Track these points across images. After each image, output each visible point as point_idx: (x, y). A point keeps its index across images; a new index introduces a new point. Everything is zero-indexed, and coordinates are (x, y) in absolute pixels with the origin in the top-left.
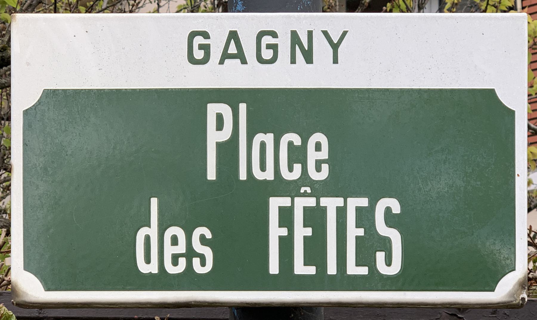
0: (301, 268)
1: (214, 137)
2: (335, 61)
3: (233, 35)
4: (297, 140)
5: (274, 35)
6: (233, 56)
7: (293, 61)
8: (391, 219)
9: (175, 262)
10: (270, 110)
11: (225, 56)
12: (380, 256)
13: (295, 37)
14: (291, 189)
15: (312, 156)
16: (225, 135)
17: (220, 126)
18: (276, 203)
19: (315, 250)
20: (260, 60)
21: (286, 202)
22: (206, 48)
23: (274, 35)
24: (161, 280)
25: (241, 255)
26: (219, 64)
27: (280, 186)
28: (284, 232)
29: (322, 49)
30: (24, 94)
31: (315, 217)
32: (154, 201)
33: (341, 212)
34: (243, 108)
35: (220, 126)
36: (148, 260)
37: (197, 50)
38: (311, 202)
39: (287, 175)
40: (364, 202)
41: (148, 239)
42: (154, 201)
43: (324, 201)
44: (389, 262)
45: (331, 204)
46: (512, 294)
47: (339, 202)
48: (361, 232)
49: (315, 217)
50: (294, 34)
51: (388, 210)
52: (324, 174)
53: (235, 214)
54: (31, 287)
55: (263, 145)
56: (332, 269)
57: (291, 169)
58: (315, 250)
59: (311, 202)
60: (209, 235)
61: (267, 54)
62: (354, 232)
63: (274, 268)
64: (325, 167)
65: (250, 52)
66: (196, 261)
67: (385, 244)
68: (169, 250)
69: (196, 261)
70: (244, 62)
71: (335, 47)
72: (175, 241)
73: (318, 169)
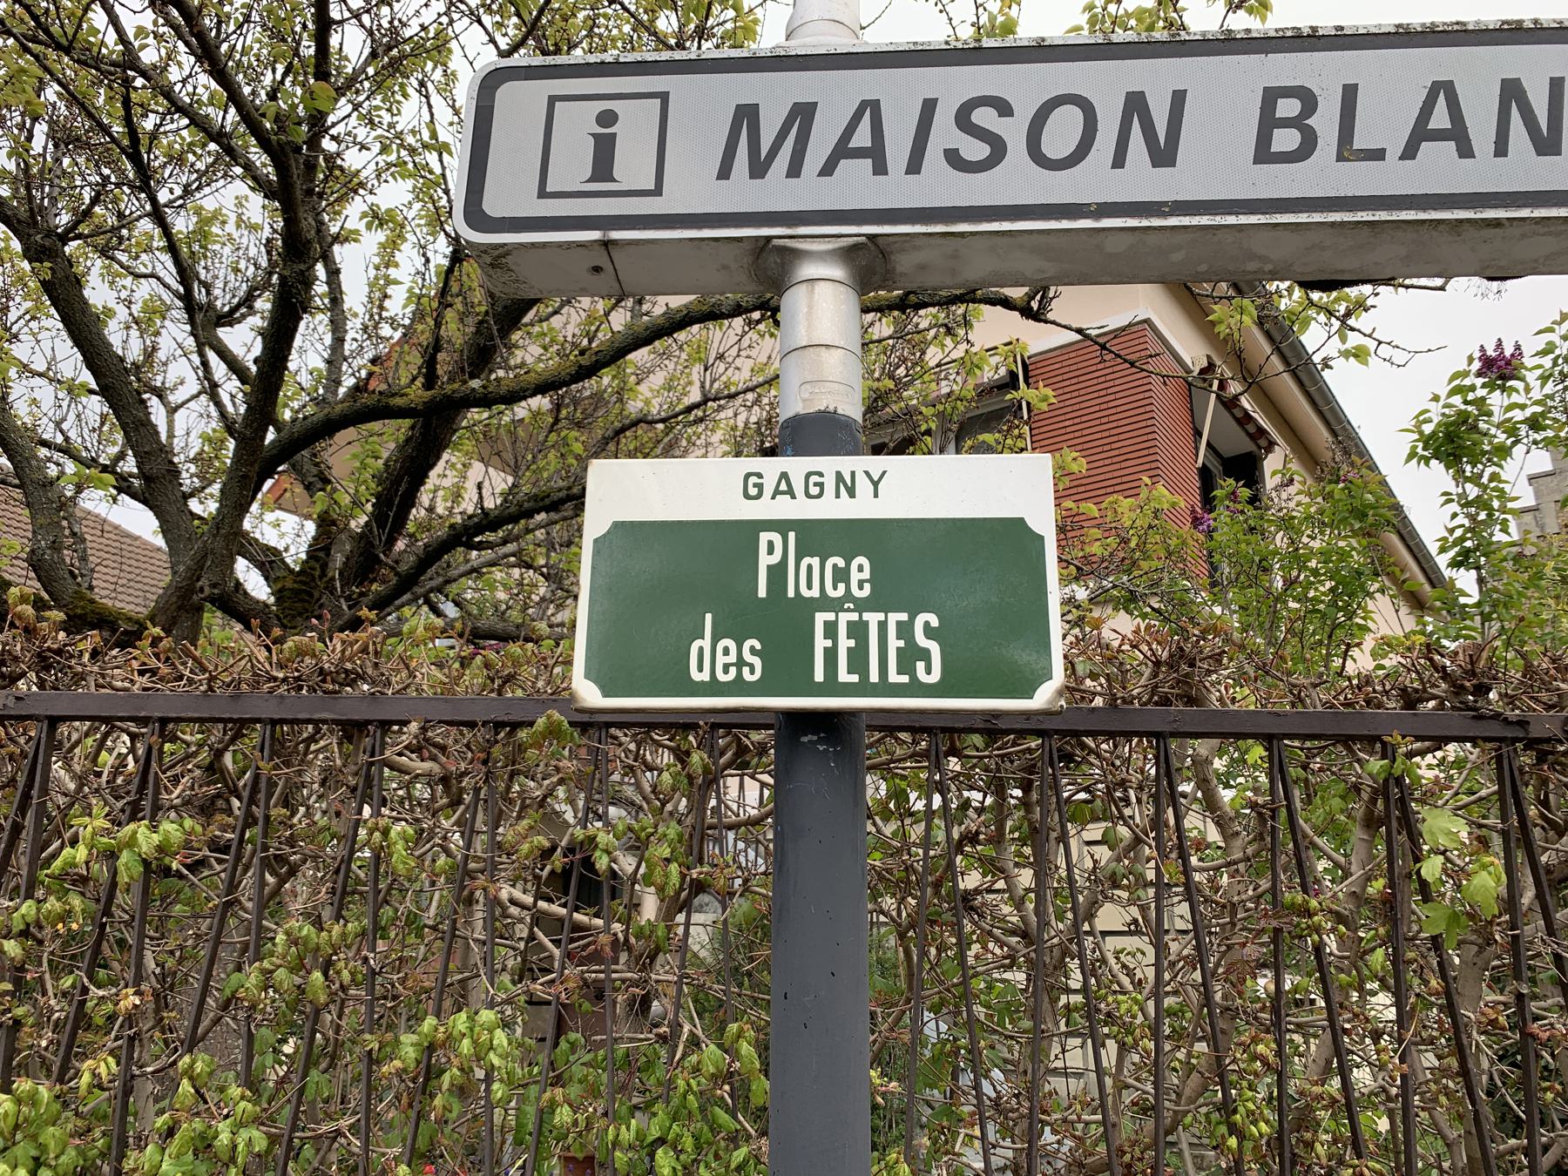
0: (844, 676)
1: (765, 561)
2: (876, 496)
3: (784, 475)
4: (841, 563)
5: (821, 474)
6: (783, 493)
7: (838, 496)
8: (929, 632)
9: (726, 671)
10: (816, 537)
11: (777, 492)
12: (920, 665)
13: (839, 475)
14: (837, 606)
15: (855, 576)
16: (776, 558)
17: (771, 551)
18: (821, 618)
19: (858, 660)
20: (808, 495)
21: (831, 616)
22: (760, 486)
23: (821, 474)
24: (713, 687)
25: (787, 664)
26: (718, 178)
27: (825, 603)
28: (829, 643)
29: (863, 486)
30: (596, 521)
31: (858, 631)
32: (709, 617)
33: (883, 626)
34: (792, 535)
35: (771, 551)
36: (700, 669)
37: (752, 489)
38: (854, 616)
39: (831, 593)
40: (904, 617)
41: (701, 649)
42: (709, 617)
43: (866, 616)
44: (929, 672)
45: (873, 618)
46: (1052, 701)
47: (881, 616)
48: (901, 643)
49: (858, 631)
50: (839, 474)
51: (927, 624)
52: (867, 590)
53: (783, 628)
54: (589, 694)
55: (810, 567)
56: (874, 677)
57: (835, 588)
58: (858, 660)
59: (854, 616)
60: (758, 646)
61: (814, 491)
62: (894, 643)
63: (819, 676)
64: (867, 586)
65: (798, 488)
66: (746, 670)
67: (925, 655)
68: (721, 659)
69: (746, 670)
70: (793, 497)
71: (876, 484)
72: (726, 651)
73: (861, 588)
